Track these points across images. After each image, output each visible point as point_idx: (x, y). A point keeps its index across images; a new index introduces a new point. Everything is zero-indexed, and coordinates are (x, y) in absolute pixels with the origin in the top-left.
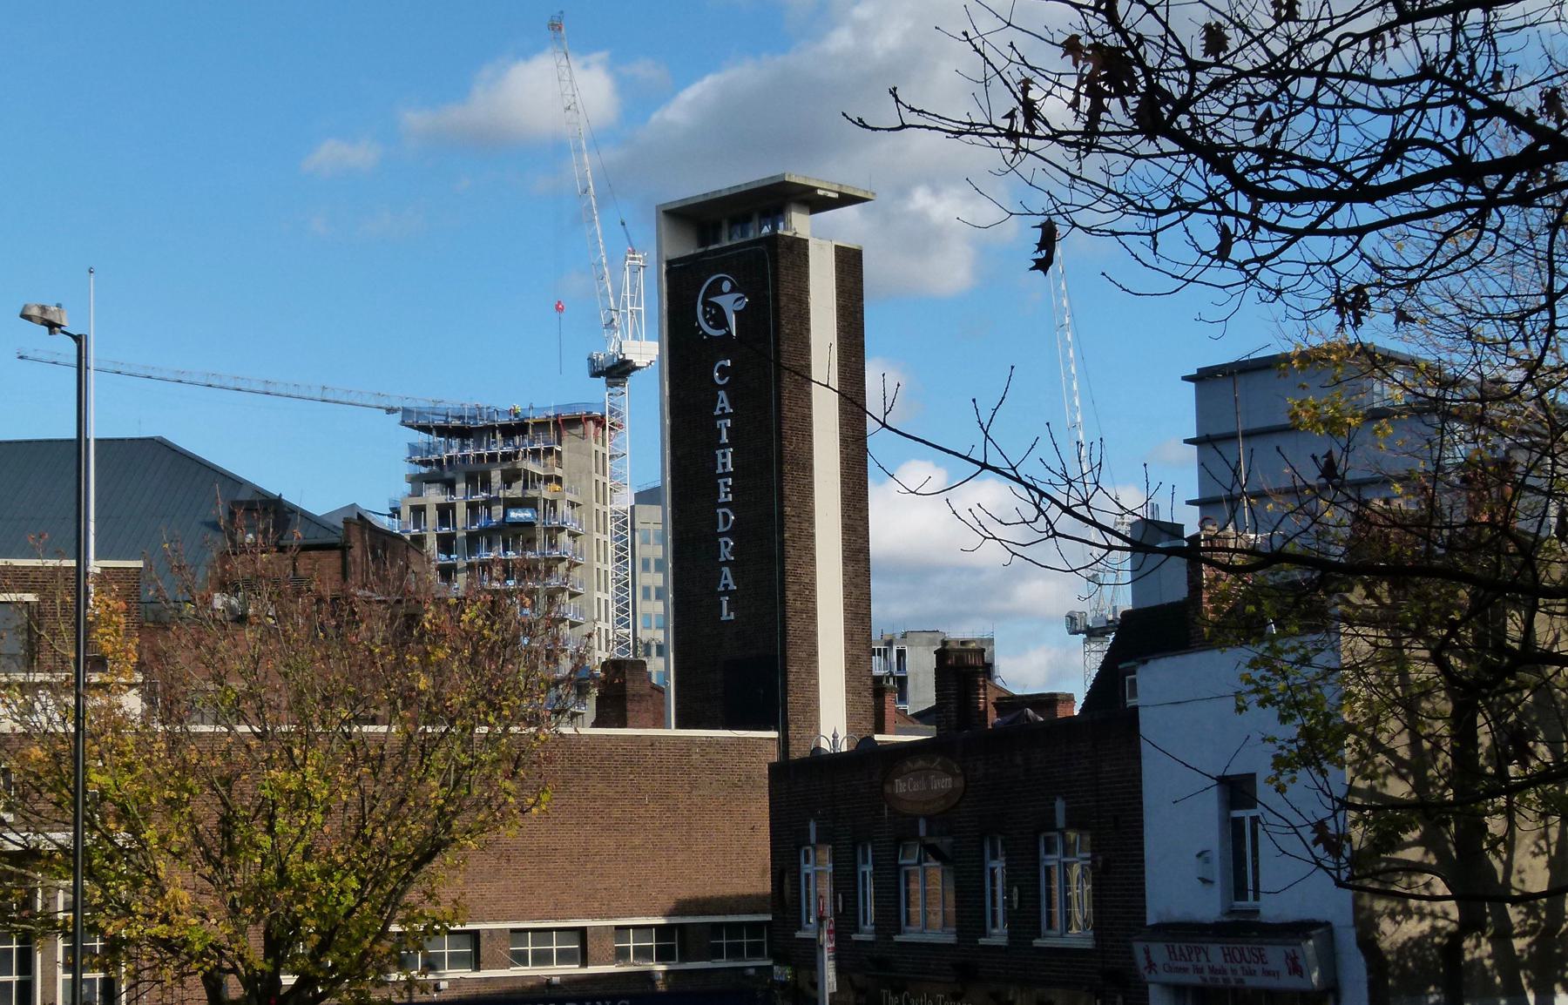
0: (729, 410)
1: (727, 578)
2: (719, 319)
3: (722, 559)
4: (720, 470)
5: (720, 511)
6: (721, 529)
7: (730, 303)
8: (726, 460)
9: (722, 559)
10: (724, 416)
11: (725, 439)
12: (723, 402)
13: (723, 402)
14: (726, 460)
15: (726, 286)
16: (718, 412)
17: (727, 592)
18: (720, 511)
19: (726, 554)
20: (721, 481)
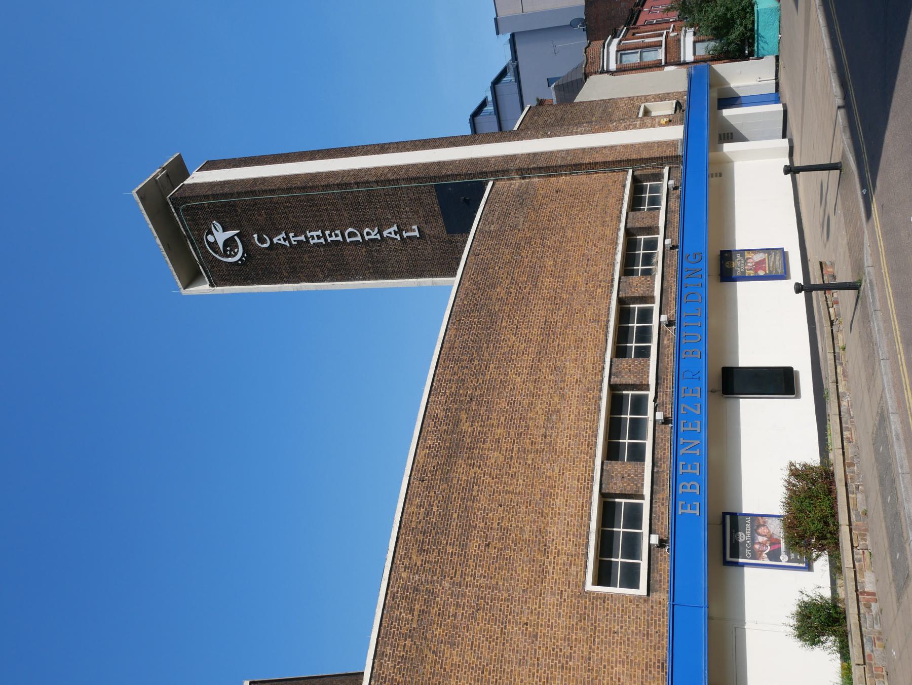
0: (283, 235)
1: (390, 232)
2: (229, 242)
3: (378, 237)
4: (322, 240)
5: (348, 240)
6: (359, 238)
7: (220, 236)
8: (314, 236)
9: (378, 237)
10: (287, 238)
11: (302, 238)
12: (279, 239)
13: (279, 239)
14: (314, 236)
15: (211, 238)
16: (287, 243)
17: (399, 231)
18: (348, 240)
19: (375, 235)
20: (329, 239)
